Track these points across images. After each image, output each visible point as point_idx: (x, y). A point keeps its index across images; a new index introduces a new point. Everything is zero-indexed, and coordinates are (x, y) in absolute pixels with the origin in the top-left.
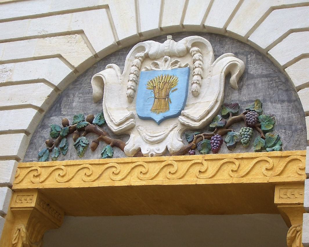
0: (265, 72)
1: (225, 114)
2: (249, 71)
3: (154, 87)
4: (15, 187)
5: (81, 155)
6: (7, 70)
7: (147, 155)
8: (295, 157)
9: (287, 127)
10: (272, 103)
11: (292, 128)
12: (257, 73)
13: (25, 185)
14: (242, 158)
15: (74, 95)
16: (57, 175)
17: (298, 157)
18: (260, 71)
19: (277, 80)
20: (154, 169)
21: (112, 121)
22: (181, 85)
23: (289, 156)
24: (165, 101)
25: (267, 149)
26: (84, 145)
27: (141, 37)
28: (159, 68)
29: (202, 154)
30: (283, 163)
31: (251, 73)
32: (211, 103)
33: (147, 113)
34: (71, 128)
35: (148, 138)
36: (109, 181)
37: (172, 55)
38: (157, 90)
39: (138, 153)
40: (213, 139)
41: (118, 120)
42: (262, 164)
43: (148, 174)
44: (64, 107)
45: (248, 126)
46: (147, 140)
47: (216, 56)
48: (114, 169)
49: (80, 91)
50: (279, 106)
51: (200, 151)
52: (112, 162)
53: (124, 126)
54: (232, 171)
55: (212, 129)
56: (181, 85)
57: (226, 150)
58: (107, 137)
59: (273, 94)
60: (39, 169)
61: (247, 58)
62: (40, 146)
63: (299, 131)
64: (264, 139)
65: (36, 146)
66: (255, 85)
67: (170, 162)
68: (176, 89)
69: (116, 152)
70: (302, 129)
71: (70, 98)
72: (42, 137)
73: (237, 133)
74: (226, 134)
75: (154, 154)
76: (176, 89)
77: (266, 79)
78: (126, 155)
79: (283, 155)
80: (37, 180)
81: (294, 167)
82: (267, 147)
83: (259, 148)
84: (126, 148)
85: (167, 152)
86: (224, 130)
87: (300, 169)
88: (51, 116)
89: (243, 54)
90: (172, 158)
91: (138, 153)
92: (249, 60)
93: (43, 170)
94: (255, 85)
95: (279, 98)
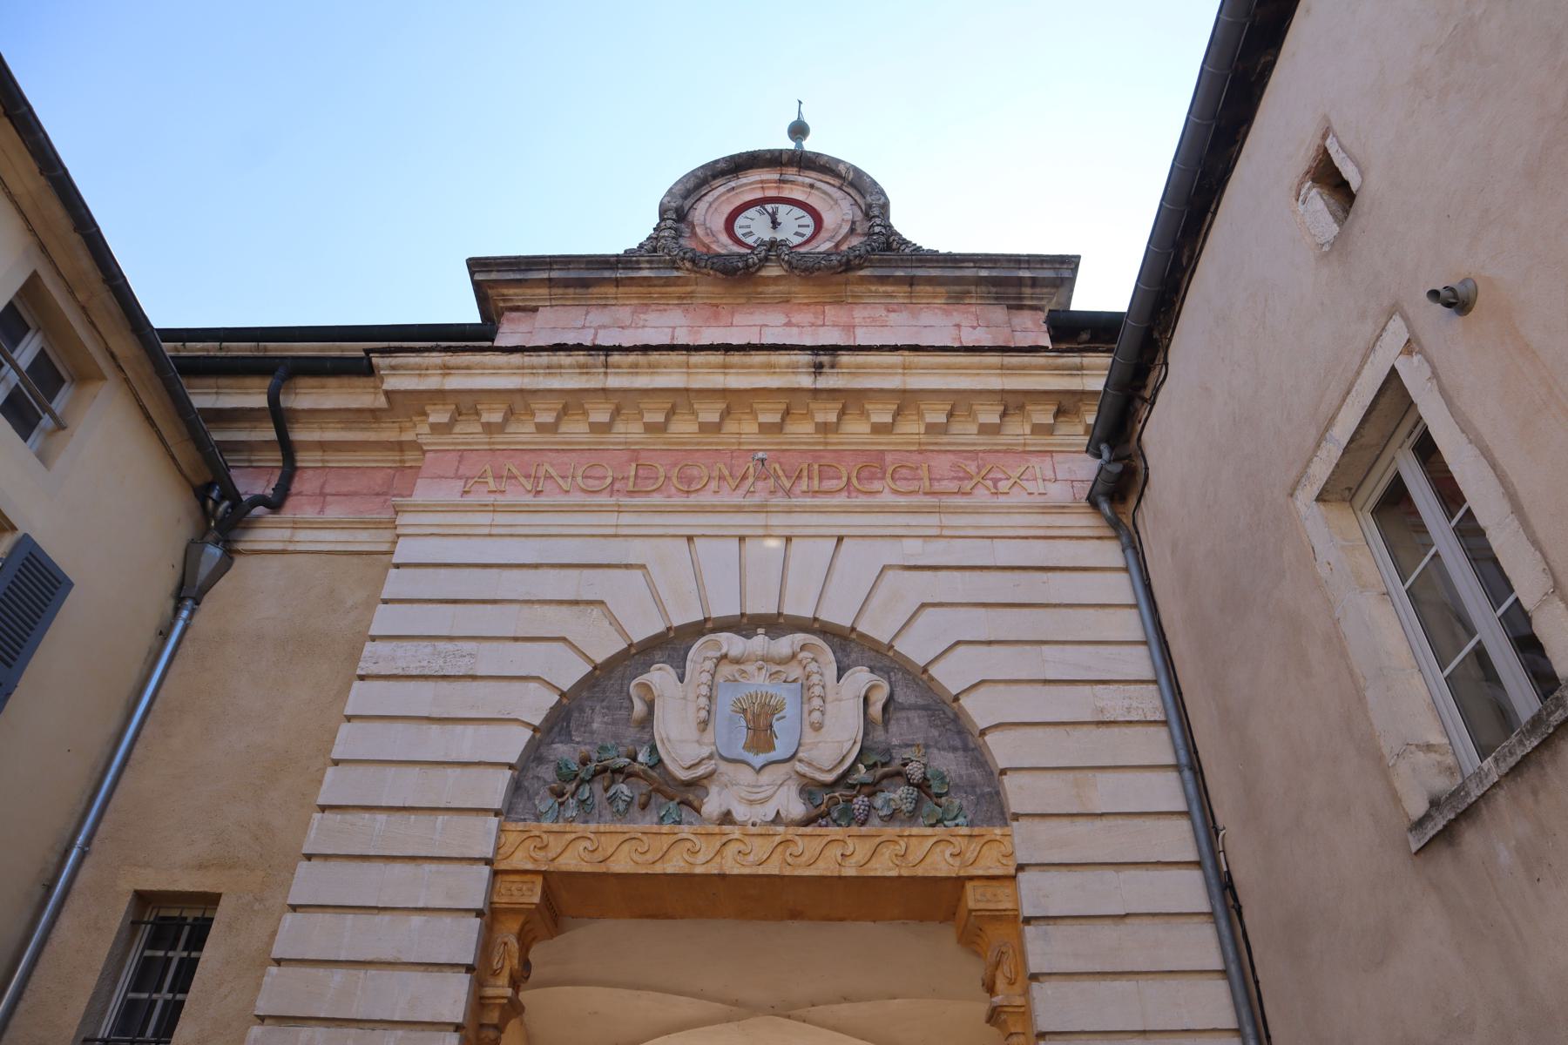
0: (921, 702)
1: (871, 762)
2: (896, 697)
3: (744, 711)
4: (503, 866)
5: (622, 815)
6: (464, 654)
7: (743, 824)
8: (993, 837)
9: (969, 789)
10: (939, 749)
11: (975, 792)
12: (908, 702)
13: (519, 861)
14: (910, 836)
15: (593, 710)
16: (581, 848)
17: (998, 838)
18: (912, 700)
19: (942, 716)
20: (760, 848)
21: (674, 760)
23: (982, 835)
24: (766, 734)
25: (946, 823)
26: (626, 798)
29: (840, 825)
30: (975, 846)
31: (900, 701)
32: (848, 745)
33: (738, 751)
34: (598, 768)
35: (742, 795)
36: (682, 864)
37: (766, 659)
38: (749, 716)
39: (727, 818)
40: (857, 803)
42: (942, 846)
43: (752, 855)
44: (576, 730)
45: (910, 784)
46: (742, 798)
48: (689, 845)
49: (604, 704)
50: (951, 755)
51: (835, 821)
52: (685, 830)
53: (701, 771)
54: (896, 855)
55: (853, 786)
56: (790, 710)
57: (877, 821)
58: (664, 787)
59: (940, 736)
60: (545, 836)
61: (889, 678)
62: (537, 794)
63: (987, 797)
64: (940, 807)
65: (528, 792)
66: (908, 719)
67: (789, 837)
68: (783, 717)
69: (685, 811)
70: (990, 793)
71: (586, 715)
72: (538, 778)
74: (871, 795)
75: (759, 821)
76: (783, 717)
77: (924, 713)
78: (704, 821)
79: (974, 834)
80: (540, 855)
82: (946, 819)
83: (934, 821)
84: (706, 810)
85: (777, 819)
86: (872, 789)
87: (1003, 856)
88: (552, 743)
89: (881, 669)
90: (792, 830)
91: (727, 818)
92: (893, 679)
93: (552, 838)
94: (908, 719)
95: (949, 743)
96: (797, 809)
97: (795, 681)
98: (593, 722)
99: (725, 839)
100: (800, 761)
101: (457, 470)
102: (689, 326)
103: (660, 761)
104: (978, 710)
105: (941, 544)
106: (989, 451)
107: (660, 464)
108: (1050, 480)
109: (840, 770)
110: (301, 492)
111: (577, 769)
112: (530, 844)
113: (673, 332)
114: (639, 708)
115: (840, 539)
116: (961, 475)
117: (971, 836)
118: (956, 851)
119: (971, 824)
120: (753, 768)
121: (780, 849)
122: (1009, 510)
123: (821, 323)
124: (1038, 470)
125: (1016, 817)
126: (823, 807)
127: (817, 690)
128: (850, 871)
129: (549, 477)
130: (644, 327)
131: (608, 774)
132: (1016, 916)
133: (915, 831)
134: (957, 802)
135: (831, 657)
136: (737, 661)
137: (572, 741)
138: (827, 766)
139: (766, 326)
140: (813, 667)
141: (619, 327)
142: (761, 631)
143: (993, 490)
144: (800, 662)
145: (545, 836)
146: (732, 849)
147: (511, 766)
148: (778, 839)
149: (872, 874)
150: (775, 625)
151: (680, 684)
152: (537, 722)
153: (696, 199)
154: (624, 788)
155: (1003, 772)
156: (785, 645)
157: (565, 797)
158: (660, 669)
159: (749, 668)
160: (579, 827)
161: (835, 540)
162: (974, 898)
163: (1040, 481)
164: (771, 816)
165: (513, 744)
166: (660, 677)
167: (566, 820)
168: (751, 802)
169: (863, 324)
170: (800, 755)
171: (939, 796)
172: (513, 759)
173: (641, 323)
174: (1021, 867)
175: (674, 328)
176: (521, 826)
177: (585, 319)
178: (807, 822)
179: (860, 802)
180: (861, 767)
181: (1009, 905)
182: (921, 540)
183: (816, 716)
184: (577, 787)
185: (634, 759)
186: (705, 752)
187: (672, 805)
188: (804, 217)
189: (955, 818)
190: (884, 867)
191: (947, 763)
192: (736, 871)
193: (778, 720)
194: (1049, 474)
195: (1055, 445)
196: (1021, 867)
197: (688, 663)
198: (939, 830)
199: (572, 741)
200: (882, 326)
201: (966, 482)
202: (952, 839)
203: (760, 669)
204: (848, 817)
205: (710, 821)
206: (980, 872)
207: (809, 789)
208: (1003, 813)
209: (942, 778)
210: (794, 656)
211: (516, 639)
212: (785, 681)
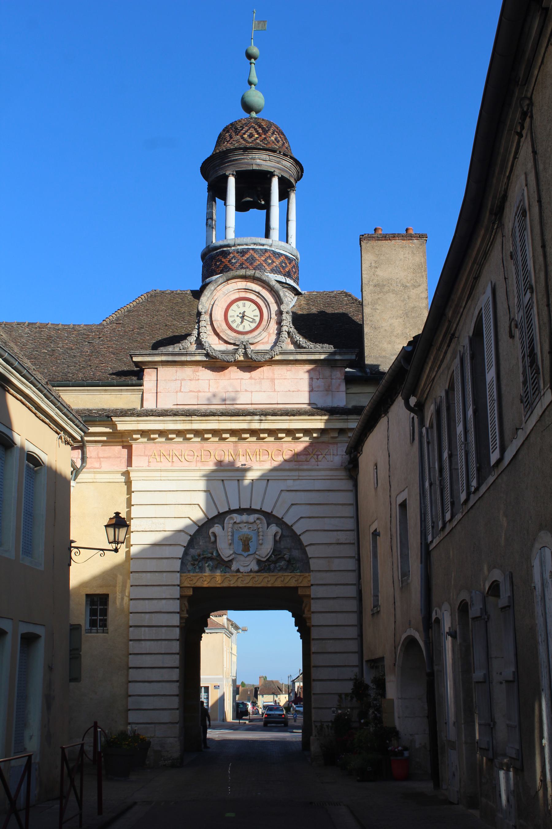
1: (275, 554)
3: (241, 539)
7: (242, 572)
13: (186, 584)
14: (285, 575)
17: (307, 576)
20: (248, 579)
25: (295, 571)
27: (230, 512)
28: (242, 530)
30: (301, 578)
32: (269, 550)
33: (240, 552)
35: (242, 564)
36: (227, 584)
37: (247, 523)
38: (243, 541)
39: (238, 571)
47: (268, 525)
48: (229, 579)
50: (297, 551)
52: (228, 575)
53: (230, 558)
55: (270, 561)
56: (254, 539)
60: (192, 577)
61: (282, 527)
67: (254, 576)
68: (252, 542)
69: (227, 569)
73: (281, 564)
75: (246, 572)
76: (252, 542)
80: (191, 582)
84: (232, 568)
85: (251, 571)
86: (275, 562)
88: (190, 549)
91: (238, 571)
96: (256, 568)
97: (255, 530)
98: (200, 542)
99: (238, 577)
100: (257, 554)
101: (145, 452)
102: (215, 379)
103: (219, 555)
104: (305, 539)
105: (298, 482)
106: (317, 443)
107: (211, 450)
108: (335, 455)
109: (267, 557)
110: (91, 457)
111: (197, 558)
112: (188, 580)
113: (209, 382)
114: (213, 539)
115: (268, 480)
116: (307, 453)
117: (300, 576)
118: (296, 579)
119: (301, 572)
120: (244, 556)
121: (252, 579)
122: (320, 470)
123: (263, 378)
124: (332, 451)
126: (263, 568)
127: (261, 534)
128: (269, 585)
130: (198, 380)
131: (206, 559)
132: (310, 596)
133: (286, 574)
134: (298, 565)
135: (265, 522)
136: (239, 523)
137: (195, 548)
138: (264, 556)
139: (243, 379)
140: (260, 526)
141: (189, 380)
142: (245, 514)
143: (317, 460)
144: (256, 524)
145: (192, 577)
146: (240, 580)
147: (180, 558)
148: (251, 577)
149: (275, 586)
150: (250, 511)
151: (223, 531)
152: (185, 545)
153: (211, 299)
154: (210, 563)
155: (310, 558)
156: (252, 518)
157: (196, 565)
158: (217, 526)
159: (241, 525)
160: (200, 574)
161: (267, 480)
162: (300, 592)
163: (332, 456)
164: (250, 570)
165: (180, 552)
166: (217, 529)
167: (197, 572)
168: (244, 566)
169: (278, 378)
170: (257, 553)
171: (293, 564)
172: (181, 557)
173: (197, 378)
174: (312, 585)
175: (209, 380)
176: (185, 574)
177: (176, 375)
179: (272, 566)
180: (273, 555)
181: (308, 593)
182: (292, 480)
183: (260, 542)
184: (198, 563)
185: (212, 554)
186: (231, 552)
187: (223, 567)
188: (256, 310)
189: (297, 570)
190: (278, 584)
191: (296, 553)
192: (241, 586)
193: (251, 542)
194: (335, 452)
195: (338, 441)
196: (312, 585)
197: (225, 524)
198: (292, 574)
199: (195, 548)
200: (285, 379)
201: (308, 456)
202: (295, 576)
203: (245, 526)
204: (269, 570)
205: (233, 572)
206: (302, 585)
207: (259, 562)
208: (310, 568)
210: (255, 521)
211: (175, 518)
212: (252, 530)
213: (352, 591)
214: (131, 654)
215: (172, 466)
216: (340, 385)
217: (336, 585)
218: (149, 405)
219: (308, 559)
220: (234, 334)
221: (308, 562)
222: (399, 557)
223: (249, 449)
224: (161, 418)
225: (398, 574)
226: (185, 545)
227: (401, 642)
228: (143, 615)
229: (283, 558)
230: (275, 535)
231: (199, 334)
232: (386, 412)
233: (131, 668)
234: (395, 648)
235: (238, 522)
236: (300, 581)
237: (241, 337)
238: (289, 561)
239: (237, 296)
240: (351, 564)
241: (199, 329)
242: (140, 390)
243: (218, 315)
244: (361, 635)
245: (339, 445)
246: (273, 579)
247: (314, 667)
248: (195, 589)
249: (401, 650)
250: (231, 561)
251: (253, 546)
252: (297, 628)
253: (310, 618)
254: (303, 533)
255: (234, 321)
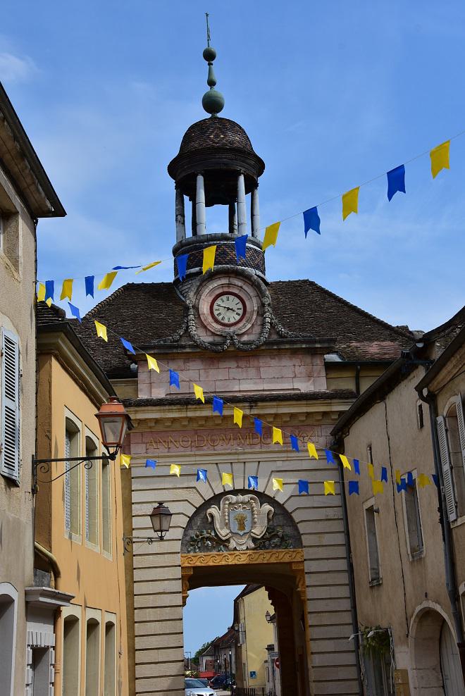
18: (279, 512)
22: (249, 519)
30: (295, 553)
33: (236, 531)
39: (235, 549)
41: (224, 535)
53: (227, 537)
74: (270, 541)
78: (230, 550)
81: (299, 555)
86: (269, 540)
91: (235, 549)
96: (253, 545)
104: (297, 517)
109: (261, 535)
115: (259, 462)
119: (294, 548)
125: (305, 547)
127: (255, 512)
129: (171, 442)
130: (189, 370)
136: (234, 504)
150: (243, 492)
155: (302, 534)
156: (246, 498)
166: (213, 510)
173: (188, 368)
174: (305, 560)
178: (254, 549)
179: (267, 543)
190: (273, 560)
191: (288, 530)
196: (305, 560)
197: (221, 506)
204: (264, 547)
207: (254, 540)
208: (302, 544)
209: (287, 535)
213: (342, 565)
214: (136, 636)
215: (168, 452)
216: (320, 371)
217: (327, 559)
218: (143, 396)
219: (300, 535)
220: (219, 327)
221: (300, 538)
222: (407, 533)
223: (240, 433)
224: (158, 408)
225: (406, 550)
226: (185, 527)
227: (415, 614)
228: (147, 596)
229: (276, 536)
230: (268, 514)
231: (187, 327)
232: (383, 398)
233: (137, 650)
234: (407, 619)
235: (233, 502)
236: (293, 557)
237: (227, 329)
238: (282, 539)
239: (220, 291)
240: (340, 539)
241: (187, 323)
242: (134, 381)
243: (204, 308)
244: (354, 607)
245: (323, 427)
246: (269, 556)
247: (311, 640)
248: (195, 568)
249: (415, 621)
250: (228, 541)
251: (248, 523)
252: (271, 601)
253: (304, 592)
254: (293, 511)
255: (219, 314)
